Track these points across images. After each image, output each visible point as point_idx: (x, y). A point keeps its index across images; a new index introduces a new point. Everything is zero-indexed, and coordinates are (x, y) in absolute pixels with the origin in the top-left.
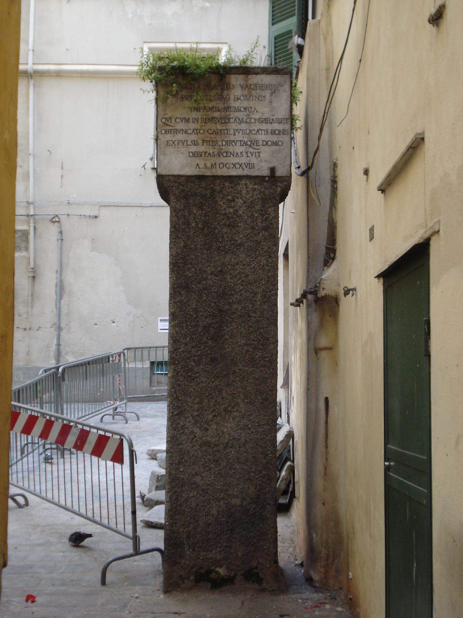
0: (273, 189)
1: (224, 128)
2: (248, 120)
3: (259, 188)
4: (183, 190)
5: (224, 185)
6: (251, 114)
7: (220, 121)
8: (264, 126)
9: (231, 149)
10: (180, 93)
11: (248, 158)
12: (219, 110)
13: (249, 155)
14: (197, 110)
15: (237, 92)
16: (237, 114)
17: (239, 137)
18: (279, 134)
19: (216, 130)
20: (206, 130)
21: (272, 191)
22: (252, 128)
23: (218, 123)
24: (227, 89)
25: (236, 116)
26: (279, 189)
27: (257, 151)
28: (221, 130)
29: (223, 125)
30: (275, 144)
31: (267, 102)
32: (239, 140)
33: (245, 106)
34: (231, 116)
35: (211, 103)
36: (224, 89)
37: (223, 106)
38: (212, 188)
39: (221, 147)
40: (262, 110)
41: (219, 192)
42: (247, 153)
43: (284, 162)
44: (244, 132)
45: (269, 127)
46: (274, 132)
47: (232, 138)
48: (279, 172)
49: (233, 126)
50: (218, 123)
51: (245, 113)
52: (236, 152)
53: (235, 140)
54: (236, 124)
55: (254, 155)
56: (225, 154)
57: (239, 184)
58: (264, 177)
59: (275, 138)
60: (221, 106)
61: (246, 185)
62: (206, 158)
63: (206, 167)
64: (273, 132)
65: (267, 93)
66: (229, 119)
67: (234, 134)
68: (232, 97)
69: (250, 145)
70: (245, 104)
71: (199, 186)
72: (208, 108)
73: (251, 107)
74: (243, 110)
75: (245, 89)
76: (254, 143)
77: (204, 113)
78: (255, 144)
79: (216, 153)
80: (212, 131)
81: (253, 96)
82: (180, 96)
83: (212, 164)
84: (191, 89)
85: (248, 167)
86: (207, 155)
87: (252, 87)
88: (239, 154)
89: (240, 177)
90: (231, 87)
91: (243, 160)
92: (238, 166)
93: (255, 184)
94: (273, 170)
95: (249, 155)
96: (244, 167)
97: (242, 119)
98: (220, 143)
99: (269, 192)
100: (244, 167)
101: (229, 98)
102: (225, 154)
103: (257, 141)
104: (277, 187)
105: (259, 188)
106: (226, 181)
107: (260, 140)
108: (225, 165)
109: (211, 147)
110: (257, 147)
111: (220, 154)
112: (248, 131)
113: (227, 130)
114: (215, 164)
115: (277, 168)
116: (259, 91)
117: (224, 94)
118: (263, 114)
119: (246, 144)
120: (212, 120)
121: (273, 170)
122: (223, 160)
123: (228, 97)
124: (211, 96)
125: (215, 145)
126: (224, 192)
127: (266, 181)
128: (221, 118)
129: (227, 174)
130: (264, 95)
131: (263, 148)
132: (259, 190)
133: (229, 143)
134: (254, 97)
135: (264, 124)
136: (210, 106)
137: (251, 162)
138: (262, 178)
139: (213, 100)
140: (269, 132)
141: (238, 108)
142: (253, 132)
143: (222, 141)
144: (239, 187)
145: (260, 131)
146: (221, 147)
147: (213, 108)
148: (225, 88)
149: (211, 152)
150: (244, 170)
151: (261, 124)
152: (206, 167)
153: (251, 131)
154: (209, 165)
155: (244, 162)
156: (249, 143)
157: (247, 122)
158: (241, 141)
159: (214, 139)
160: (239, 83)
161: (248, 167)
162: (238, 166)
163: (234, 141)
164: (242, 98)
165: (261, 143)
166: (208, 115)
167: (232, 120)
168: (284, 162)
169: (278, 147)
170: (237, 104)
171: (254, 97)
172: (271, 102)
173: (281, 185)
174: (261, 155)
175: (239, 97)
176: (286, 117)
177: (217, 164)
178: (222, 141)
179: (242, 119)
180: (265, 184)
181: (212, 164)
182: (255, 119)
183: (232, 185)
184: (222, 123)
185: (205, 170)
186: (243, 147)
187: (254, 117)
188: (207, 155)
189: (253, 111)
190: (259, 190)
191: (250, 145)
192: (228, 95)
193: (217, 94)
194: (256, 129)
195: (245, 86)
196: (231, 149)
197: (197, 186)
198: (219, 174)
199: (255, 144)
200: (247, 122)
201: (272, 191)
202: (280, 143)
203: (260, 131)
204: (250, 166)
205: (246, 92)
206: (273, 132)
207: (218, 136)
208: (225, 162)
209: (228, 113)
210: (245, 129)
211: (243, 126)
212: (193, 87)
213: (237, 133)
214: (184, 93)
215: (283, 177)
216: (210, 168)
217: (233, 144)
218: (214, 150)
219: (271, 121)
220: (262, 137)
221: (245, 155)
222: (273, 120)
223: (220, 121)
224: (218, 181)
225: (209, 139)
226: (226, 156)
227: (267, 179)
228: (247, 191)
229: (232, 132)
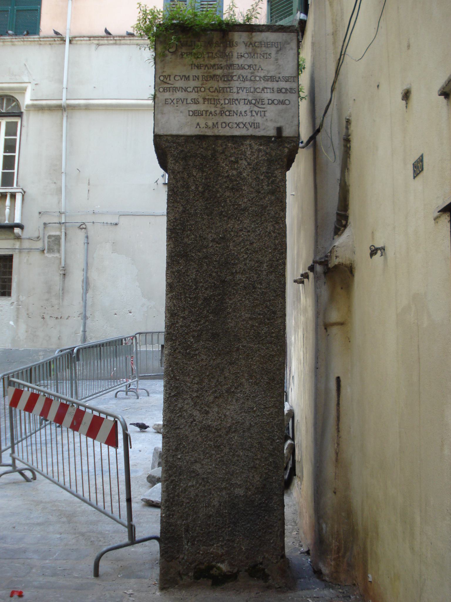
0: (280, 150)
1: (227, 86)
2: (253, 78)
3: (265, 148)
4: (182, 151)
5: (226, 145)
6: (256, 71)
8: (270, 85)
9: (234, 107)
10: (180, 50)
11: (253, 118)
12: (222, 67)
13: (254, 113)
14: (199, 67)
15: (241, 49)
16: (240, 72)
17: (243, 95)
19: (218, 88)
20: (208, 87)
22: (257, 87)
24: (230, 46)
25: (239, 74)
26: (286, 150)
29: (225, 83)
30: (282, 102)
31: (272, 59)
33: (249, 64)
34: (234, 74)
37: (225, 64)
38: (214, 149)
39: (223, 105)
40: (268, 67)
41: (222, 153)
42: (251, 111)
43: (292, 122)
45: (275, 85)
46: (281, 90)
47: (235, 96)
48: (287, 132)
49: (236, 84)
50: (220, 81)
51: (249, 70)
52: (239, 111)
54: (240, 82)
55: (259, 114)
56: (227, 113)
57: (243, 144)
58: (270, 137)
59: (281, 97)
60: (224, 63)
62: (208, 117)
63: (207, 126)
64: (280, 91)
65: (273, 51)
66: (232, 77)
67: (238, 93)
68: (235, 55)
69: (254, 104)
70: (250, 62)
72: (209, 66)
73: (256, 65)
74: (246, 67)
75: (249, 46)
76: (259, 102)
77: (205, 71)
78: (260, 103)
79: (218, 112)
80: (214, 88)
81: (257, 54)
82: (180, 53)
85: (253, 127)
86: (208, 114)
87: (256, 44)
88: (243, 113)
89: (244, 138)
90: (234, 44)
91: (247, 119)
93: (261, 145)
94: (279, 130)
97: (247, 76)
98: (222, 102)
99: (276, 153)
100: (248, 126)
101: (232, 55)
102: (227, 113)
103: (262, 100)
104: (284, 147)
106: (228, 141)
110: (263, 106)
111: (222, 113)
112: (252, 90)
114: (217, 123)
115: (284, 128)
116: (264, 49)
117: (227, 51)
118: (268, 72)
119: (251, 103)
121: (279, 130)
122: (227, 119)
123: (231, 54)
124: (213, 53)
125: (217, 104)
126: (226, 153)
127: (272, 142)
128: (223, 76)
130: (269, 52)
131: (269, 106)
132: (265, 151)
133: (232, 101)
134: (259, 55)
135: (269, 82)
139: (215, 58)
140: (275, 90)
141: (242, 65)
142: (258, 90)
144: (243, 148)
145: (265, 90)
146: (223, 105)
147: (214, 65)
149: (213, 110)
151: (266, 82)
152: (207, 126)
154: (210, 124)
155: (248, 121)
158: (245, 99)
159: (216, 98)
160: (242, 40)
161: (253, 127)
163: (237, 100)
164: (246, 55)
166: (209, 73)
169: (284, 106)
170: (241, 62)
171: (259, 55)
172: (277, 60)
173: (288, 146)
174: (267, 114)
175: (242, 54)
177: (219, 124)
178: (225, 99)
179: (247, 76)
180: (271, 144)
181: (213, 123)
182: (260, 77)
184: (224, 81)
185: (206, 130)
187: (259, 74)
188: (208, 114)
189: (257, 68)
190: (265, 151)
191: (254, 104)
192: (231, 52)
193: (219, 51)
194: (261, 87)
195: (249, 43)
196: (234, 107)
197: (197, 147)
198: (222, 134)
199: (260, 103)
200: (251, 80)
202: (287, 102)
203: (265, 90)
205: (250, 50)
206: (280, 91)
207: (221, 94)
208: (228, 122)
209: (231, 71)
210: (249, 87)
211: (247, 84)
213: (240, 91)
214: (184, 50)
218: (216, 109)
219: (277, 79)
220: (267, 96)
221: (249, 114)
222: (279, 78)
223: (223, 79)
224: (220, 142)
225: (210, 97)
226: (229, 115)
227: (273, 139)
228: (252, 152)
229: (235, 90)
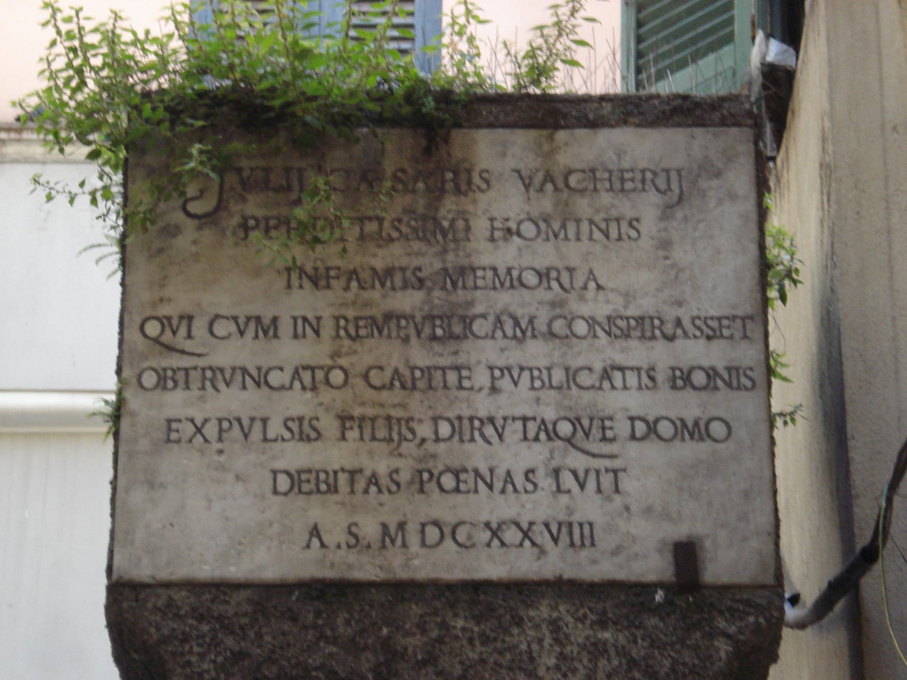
0: (696, 648)
1: (443, 361)
2: (559, 326)
3: (622, 640)
4: (239, 656)
5: (444, 625)
6: (572, 297)
7: (427, 331)
8: (636, 353)
9: (477, 455)
10: (235, 207)
11: (564, 499)
12: (421, 281)
13: (568, 481)
14: (318, 279)
15: (506, 202)
16: (505, 299)
17: (516, 400)
18: (710, 386)
19: (407, 373)
20: (361, 368)
21: (687, 657)
22: (579, 362)
23: (414, 340)
24: (458, 191)
25: (500, 306)
26: (723, 648)
27: (607, 463)
28: (428, 371)
29: (437, 347)
30: (696, 431)
31: (645, 243)
32: (518, 411)
33: (541, 263)
34: (479, 309)
35: (381, 252)
36: (443, 191)
37: (438, 265)
38: (386, 644)
39: (430, 446)
40: (627, 278)
41: (424, 663)
42: (556, 472)
43: (743, 517)
44: (540, 380)
45: (661, 355)
46: (687, 378)
47: (483, 406)
48: (723, 565)
49: (484, 352)
50: (414, 340)
51: (542, 294)
52: (501, 472)
53: (499, 415)
54: (502, 343)
55: (591, 484)
56: (448, 481)
57: (519, 622)
58: (643, 589)
59: (689, 405)
60: (430, 262)
61: (555, 625)
62: (359, 497)
63: (355, 540)
64: (681, 379)
65: (647, 207)
66: (467, 321)
67: (494, 390)
68: (480, 226)
69: (569, 440)
70: (545, 254)
71: (322, 636)
72: (366, 275)
73: (571, 270)
74: (531, 279)
75: (541, 190)
76: (588, 428)
77: (350, 296)
78: (596, 433)
79: (404, 476)
80: (388, 373)
81: (578, 221)
82: (236, 220)
83: (385, 526)
84: (289, 188)
85: (564, 539)
86: (360, 485)
87: (573, 180)
88: (519, 480)
89: (523, 590)
90: (476, 180)
91: (539, 506)
92: (512, 535)
93: (602, 624)
94: (686, 554)
95: (568, 481)
96: (543, 538)
97: (531, 321)
98: (424, 430)
99: (675, 662)
100: (543, 538)
101: (468, 229)
102: (448, 481)
103: (604, 421)
104: (711, 635)
105: (622, 640)
106: (452, 606)
107: (619, 416)
108: (449, 531)
109: (383, 447)
110: (606, 448)
111: (423, 480)
112: (558, 376)
113: (458, 368)
114: (402, 526)
115: (708, 544)
116: (606, 198)
117: (442, 212)
118: (628, 297)
119: (552, 435)
120: (385, 323)
121: (686, 554)
122: (444, 508)
123: (460, 224)
124: (380, 220)
125: (402, 438)
126: (445, 662)
127: (655, 610)
128: (430, 318)
129: (458, 574)
130: (630, 213)
131: (633, 449)
132: (622, 652)
133: (466, 428)
134: (585, 227)
135: (634, 343)
136: (379, 264)
137: (577, 517)
138: (634, 594)
139: (391, 240)
140: (661, 377)
141: (509, 271)
142: (585, 379)
143: (435, 420)
144: (521, 639)
145: (617, 376)
146: (430, 446)
147: (389, 272)
148: (449, 186)
149: (382, 468)
150: (543, 552)
151: (621, 343)
152: (355, 540)
153: (571, 374)
154: (370, 529)
155: (540, 515)
156: (565, 428)
157: (552, 335)
158: (525, 419)
159: (396, 413)
160: (511, 162)
161: (564, 539)
162: (512, 535)
163: (491, 420)
164: (528, 229)
165: (622, 428)
166: (367, 304)
167: (479, 327)
168: (743, 517)
169: (704, 448)
170: (507, 255)
171: (585, 227)
172: (665, 245)
173: (732, 630)
174: (626, 483)
175: (513, 225)
176: (740, 312)
177: (412, 528)
178: (435, 420)
179: (531, 321)
180: (653, 621)
181: (385, 526)
182: (592, 322)
183: (487, 627)
184: (434, 338)
185: (352, 557)
186: (537, 447)
187: (585, 309)
188: (360, 485)
189: (579, 282)
190: (622, 652)
191: (569, 440)
192: (463, 214)
193: (409, 211)
194: (598, 366)
195: (540, 176)
196: (477, 455)
197: (311, 635)
198: (422, 574)
199: (596, 433)
200: (552, 335)
201: (687, 657)
202: (717, 429)
203: (617, 376)
204: (574, 534)
205: (546, 203)
206: (681, 379)
207: (417, 395)
208: (449, 518)
209: (461, 295)
210: (542, 363)
211: (536, 352)
212: (295, 183)
213: (505, 383)
214: (254, 206)
215: (739, 587)
216: (376, 545)
217: (489, 431)
218: (397, 463)
219: (669, 328)
220: (625, 401)
221: (546, 483)
222: (678, 323)
223: (427, 331)
224: (416, 610)
225: (370, 412)
226: (457, 490)
227: (659, 596)
228: (562, 656)
229: (482, 378)
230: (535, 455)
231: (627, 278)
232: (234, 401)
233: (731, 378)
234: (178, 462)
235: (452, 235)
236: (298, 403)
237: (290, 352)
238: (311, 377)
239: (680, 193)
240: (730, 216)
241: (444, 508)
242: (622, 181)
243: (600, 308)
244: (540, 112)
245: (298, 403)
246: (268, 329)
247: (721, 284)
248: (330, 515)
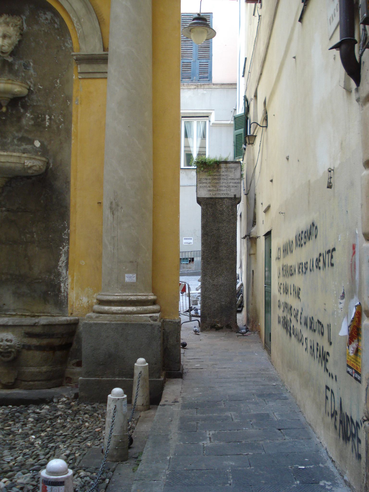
8: (232, 181)
9: (221, 188)
16: (223, 177)
17: (224, 185)
30: (236, 187)
40: (232, 175)
45: (234, 181)
47: (222, 185)
48: (237, 196)
49: (222, 181)
59: (236, 185)
60: (218, 174)
63: (213, 195)
64: (235, 183)
70: (226, 173)
76: (229, 187)
91: (225, 192)
94: (235, 195)
111: (217, 190)
121: (235, 195)
122: (219, 192)
133: (220, 186)
144: (224, 201)
152: (213, 195)
154: (214, 194)
170: (223, 174)
196: (221, 188)
205: (226, 170)
206: (235, 183)
211: (225, 181)
214: (206, 170)
220: (231, 184)
230: (225, 188)
231: (232, 175)
232: (205, 185)
233: (239, 183)
234: (201, 189)
235: (219, 172)
236: (209, 185)
237: (208, 181)
238: (210, 183)
239: (235, 169)
240: (239, 170)
241: (219, 192)
242: (231, 168)
243: (230, 178)
244: (226, 162)
245: (209, 185)
246: (207, 179)
247: (238, 176)
248: (211, 193)
